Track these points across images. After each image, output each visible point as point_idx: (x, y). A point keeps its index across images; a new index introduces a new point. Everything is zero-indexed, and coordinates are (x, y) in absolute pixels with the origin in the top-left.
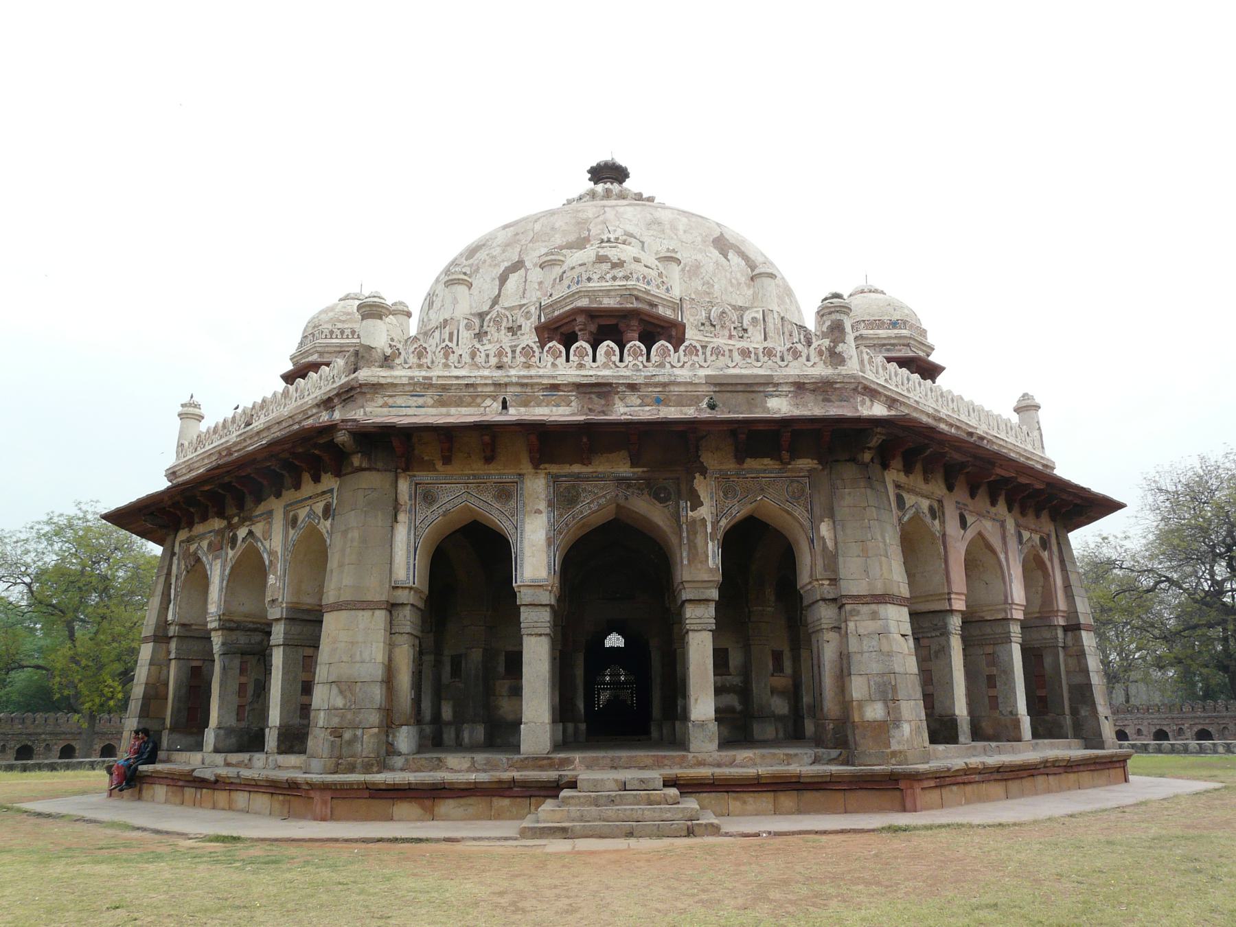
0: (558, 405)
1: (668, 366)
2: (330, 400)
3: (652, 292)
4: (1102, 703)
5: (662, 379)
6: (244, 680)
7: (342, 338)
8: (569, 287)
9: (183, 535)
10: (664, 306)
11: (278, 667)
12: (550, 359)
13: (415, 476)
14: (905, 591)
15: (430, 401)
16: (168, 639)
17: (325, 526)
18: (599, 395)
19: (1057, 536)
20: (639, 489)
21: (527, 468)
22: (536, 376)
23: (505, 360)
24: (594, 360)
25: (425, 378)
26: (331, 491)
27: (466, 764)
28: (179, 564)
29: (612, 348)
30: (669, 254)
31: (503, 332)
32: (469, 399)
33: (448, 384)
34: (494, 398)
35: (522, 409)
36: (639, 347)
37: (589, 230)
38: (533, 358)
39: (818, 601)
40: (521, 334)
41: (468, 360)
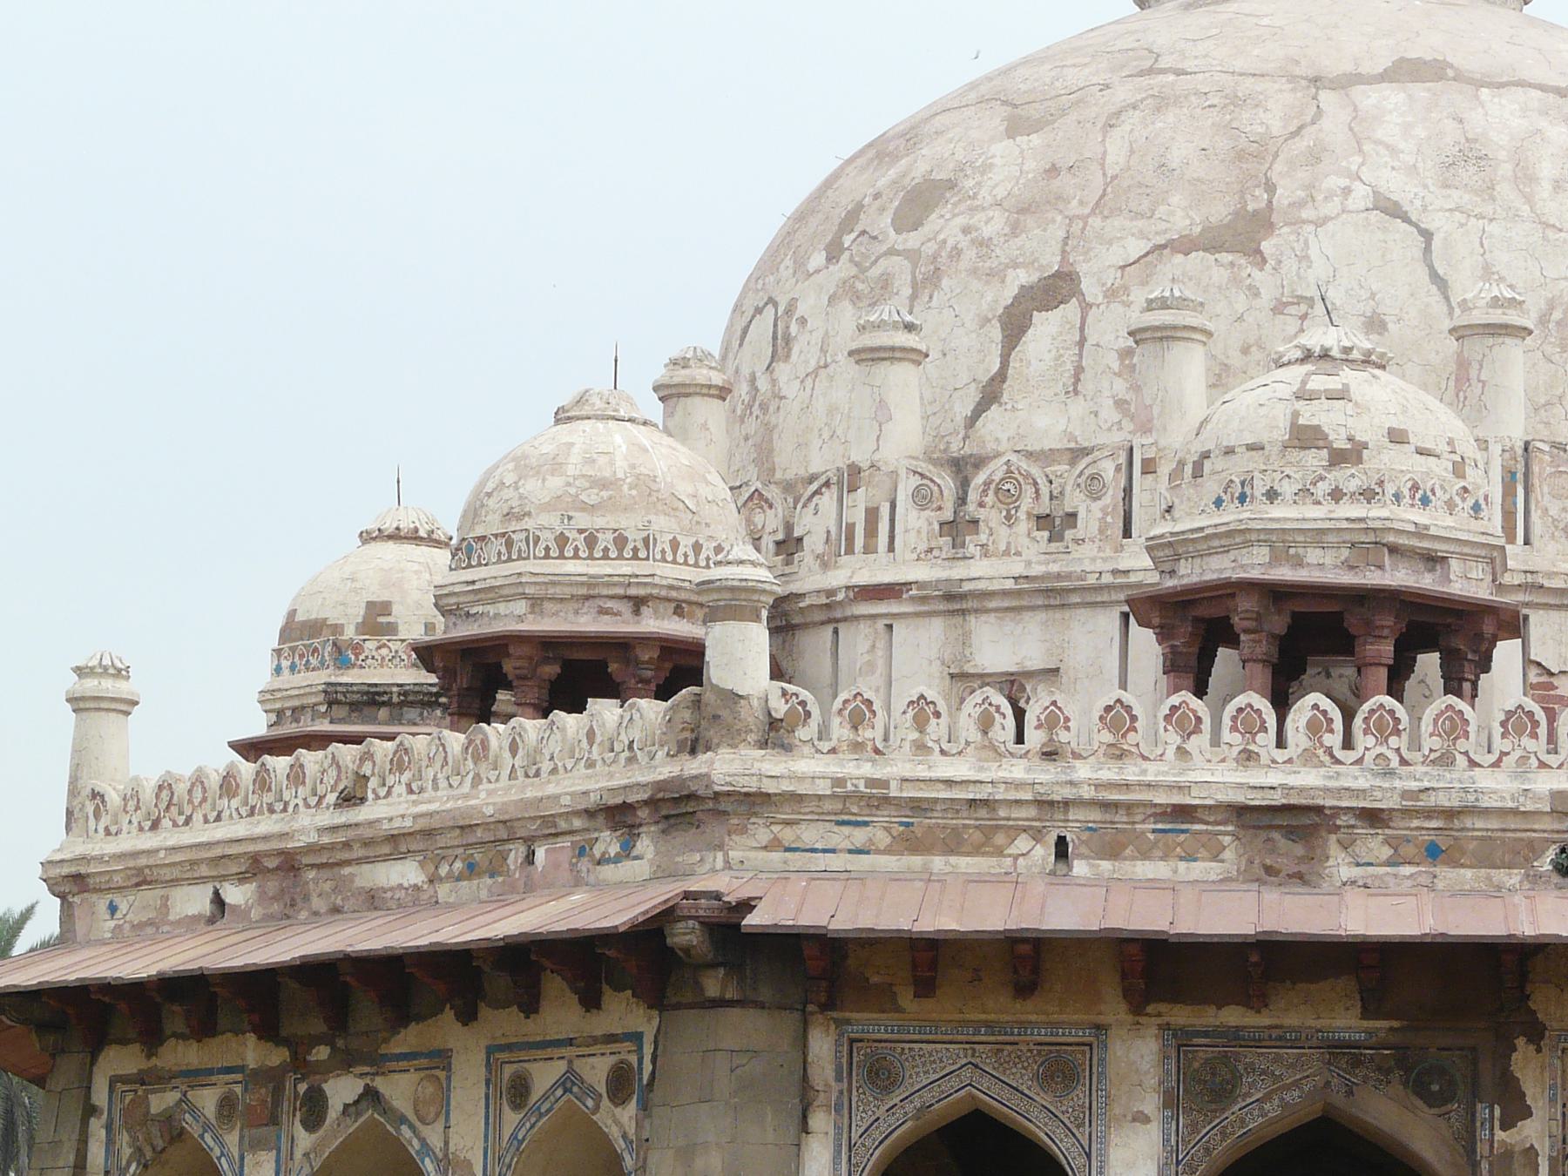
0: (1190, 858)
1: (1461, 761)
3: (1433, 531)
5: (1443, 800)
7: (591, 557)
8: (1218, 503)
10: (1464, 557)
12: (1174, 738)
13: (848, 1022)
15: (883, 839)
17: (619, 1121)
18: (1292, 833)
20: (1379, 1069)
21: (1114, 1010)
22: (1140, 784)
23: (1063, 736)
24: (1281, 743)
25: (871, 782)
28: (110, 1142)
29: (1324, 713)
30: (1497, 317)
31: (1023, 526)
32: (977, 836)
33: (926, 799)
34: (1037, 835)
35: (1106, 865)
36: (1392, 712)
37: (1271, 188)
38: (1131, 735)
40: (1077, 541)
41: (975, 735)
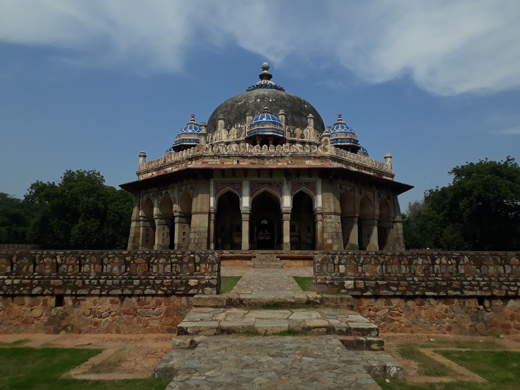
2: (191, 158)
4: (402, 243)
6: (164, 232)
9: (143, 192)
11: (177, 228)
12: (250, 150)
14: (339, 212)
16: (140, 221)
18: (263, 159)
19: (393, 196)
23: (238, 149)
26: (192, 183)
27: (228, 252)
39: (317, 214)
